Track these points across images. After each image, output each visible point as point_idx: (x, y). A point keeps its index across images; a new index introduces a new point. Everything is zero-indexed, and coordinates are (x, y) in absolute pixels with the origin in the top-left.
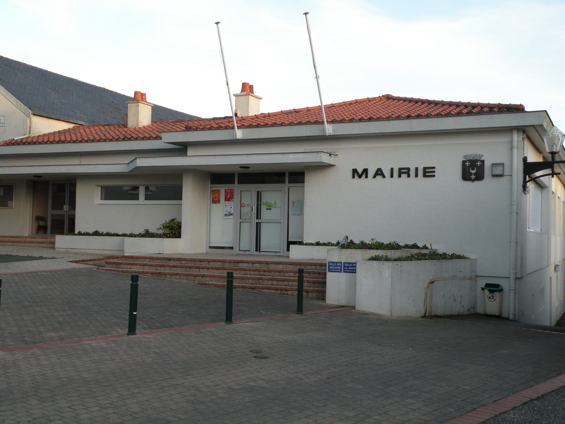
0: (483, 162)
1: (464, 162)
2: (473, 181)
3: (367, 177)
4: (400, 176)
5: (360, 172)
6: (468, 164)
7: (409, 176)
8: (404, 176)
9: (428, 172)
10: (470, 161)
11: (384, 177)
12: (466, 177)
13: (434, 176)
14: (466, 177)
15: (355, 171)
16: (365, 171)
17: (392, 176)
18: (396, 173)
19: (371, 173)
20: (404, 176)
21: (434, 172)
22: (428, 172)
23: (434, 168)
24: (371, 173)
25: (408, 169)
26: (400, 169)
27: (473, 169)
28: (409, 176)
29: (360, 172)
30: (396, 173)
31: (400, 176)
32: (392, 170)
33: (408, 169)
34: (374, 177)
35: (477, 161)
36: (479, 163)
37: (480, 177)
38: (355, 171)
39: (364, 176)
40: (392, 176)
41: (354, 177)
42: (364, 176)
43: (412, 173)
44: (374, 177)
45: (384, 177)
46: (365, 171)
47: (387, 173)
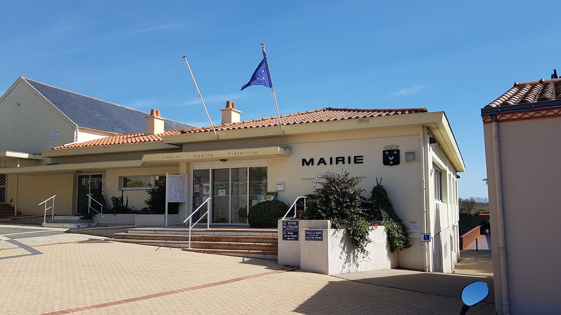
0: (398, 151)
1: (384, 152)
2: (391, 165)
3: (313, 164)
4: (337, 163)
5: (308, 161)
6: (387, 153)
7: (344, 163)
8: (340, 163)
9: (358, 160)
10: (388, 151)
11: (325, 164)
13: (362, 162)
14: (386, 162)
15: (304, 161)
16: (312, 160)
17: (331, 163)
18: (334, 161)
19: (316, 161)
20: (340, 163)
21: (362, 159)
22: (358, 160)
23: (362, 156)
24: (316, 161)
25: (343, 158)
26: (337, 158)
27: (391, 157)
28: (344, 163)
29: (308, 161)
31: (337, 163)
32: (331, 159)
33: (343, 158)
34: (318, 164)
35: (394, 151)
36: (395, 152)
37: (397, 162)
38: (304, 161)
39: (311, 163)
40: (331, 163)
41: (303, 165)
42: (311, 163)
43: (346, 160)
44: (318, 164)
45: (325, 164)
46: (312, 160)
47: (327, 161)
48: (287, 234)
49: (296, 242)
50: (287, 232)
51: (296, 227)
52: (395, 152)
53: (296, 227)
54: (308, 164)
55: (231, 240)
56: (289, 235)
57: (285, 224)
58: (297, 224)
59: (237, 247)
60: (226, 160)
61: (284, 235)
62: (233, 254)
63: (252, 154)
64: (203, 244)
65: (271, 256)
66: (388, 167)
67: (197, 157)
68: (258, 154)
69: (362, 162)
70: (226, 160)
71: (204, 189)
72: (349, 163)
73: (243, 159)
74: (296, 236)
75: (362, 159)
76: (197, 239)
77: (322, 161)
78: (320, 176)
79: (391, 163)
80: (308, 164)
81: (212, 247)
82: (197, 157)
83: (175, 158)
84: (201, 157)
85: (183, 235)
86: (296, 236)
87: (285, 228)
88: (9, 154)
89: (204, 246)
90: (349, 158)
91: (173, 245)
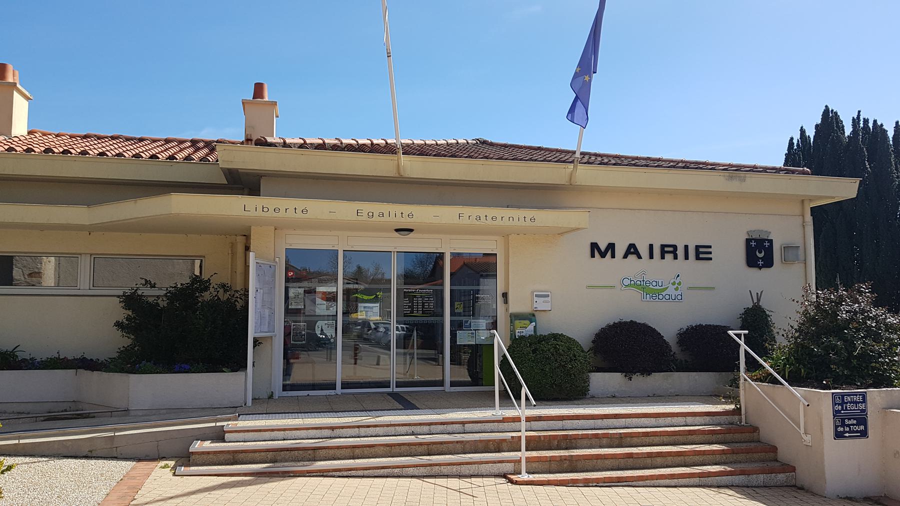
0: (771, 241)
1: (748, 241)
2: (760, 268)
3: (613, 256)
4: (663, 257)
5: (603, 247)
6: (753, 244)
7: (676, 257)
8: (669, 257)
9: (702, 253)
10: (756, 240)
11: (640, 257)
12: (768, 262)
13: (711, 259)
14: (752, 261)
15: (594, 246)
16: (611, 247)
17: (651, 257)
18: (657, 252)
19: (620, 250)
20: (669, 257)
21: (711, 253)
22: (702, 253)
23: (710, 247)
24: (620, 250)
25: (675, 247)
26: (697, 247)
27: (760, 252)
28: (676, 257)
29: (603, 247)
30: (657, 252)
31: (663, 257)
32: (651, 246)
33: (675, 247)
34: (625, 257)
35: (764, 240)
36: (767, 244)
37: (768, 262)
38: (594, 246)
39: (609, 254)
40: (651, 257)
41: (593, 256)
42: (609, 254)
43: (680, 252)
44: (625, 257)
45: (640, 257)
46: (611, 247)
47: (644, 251)
48: (843, 425)
49: (863, 440)
50: (843, 420)
51: (862, 406)
52: (753, 244)
53: (862, 406)
54: (603, 255)
55: (605, 441)
56: (848, 426)
57: (838, 401)
58: (864, 401)
59: (649, 461)
60: (411, 230)
61: (836, 427)
62: (667, 482)
63: (522, 223)
64: (562, 459)
65: (762, 477)
66: (754, 271)
67: (365, 217)
68: (537, 223)
69: (711, 259)
70: (411, 230)
71: (319, 301)
72: (687, 258)
73: (449, 229)
74: (862, 427)
75: (711, 253)
76: (504, 445)
77: (632, 250)
78: (627, 282)
79: (761, 263)
80: (603, 255)
81: (580, 465)
82: (365, 217)
83: (291, 214)
84: (376, 218)
85: (458, 437)
86: (862, 427)
87: (839, 411)
88: (862, 125)
89: (554, 466)
90: (686, 247)
91: (473, 469)
